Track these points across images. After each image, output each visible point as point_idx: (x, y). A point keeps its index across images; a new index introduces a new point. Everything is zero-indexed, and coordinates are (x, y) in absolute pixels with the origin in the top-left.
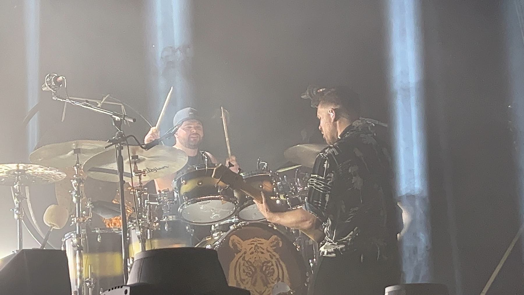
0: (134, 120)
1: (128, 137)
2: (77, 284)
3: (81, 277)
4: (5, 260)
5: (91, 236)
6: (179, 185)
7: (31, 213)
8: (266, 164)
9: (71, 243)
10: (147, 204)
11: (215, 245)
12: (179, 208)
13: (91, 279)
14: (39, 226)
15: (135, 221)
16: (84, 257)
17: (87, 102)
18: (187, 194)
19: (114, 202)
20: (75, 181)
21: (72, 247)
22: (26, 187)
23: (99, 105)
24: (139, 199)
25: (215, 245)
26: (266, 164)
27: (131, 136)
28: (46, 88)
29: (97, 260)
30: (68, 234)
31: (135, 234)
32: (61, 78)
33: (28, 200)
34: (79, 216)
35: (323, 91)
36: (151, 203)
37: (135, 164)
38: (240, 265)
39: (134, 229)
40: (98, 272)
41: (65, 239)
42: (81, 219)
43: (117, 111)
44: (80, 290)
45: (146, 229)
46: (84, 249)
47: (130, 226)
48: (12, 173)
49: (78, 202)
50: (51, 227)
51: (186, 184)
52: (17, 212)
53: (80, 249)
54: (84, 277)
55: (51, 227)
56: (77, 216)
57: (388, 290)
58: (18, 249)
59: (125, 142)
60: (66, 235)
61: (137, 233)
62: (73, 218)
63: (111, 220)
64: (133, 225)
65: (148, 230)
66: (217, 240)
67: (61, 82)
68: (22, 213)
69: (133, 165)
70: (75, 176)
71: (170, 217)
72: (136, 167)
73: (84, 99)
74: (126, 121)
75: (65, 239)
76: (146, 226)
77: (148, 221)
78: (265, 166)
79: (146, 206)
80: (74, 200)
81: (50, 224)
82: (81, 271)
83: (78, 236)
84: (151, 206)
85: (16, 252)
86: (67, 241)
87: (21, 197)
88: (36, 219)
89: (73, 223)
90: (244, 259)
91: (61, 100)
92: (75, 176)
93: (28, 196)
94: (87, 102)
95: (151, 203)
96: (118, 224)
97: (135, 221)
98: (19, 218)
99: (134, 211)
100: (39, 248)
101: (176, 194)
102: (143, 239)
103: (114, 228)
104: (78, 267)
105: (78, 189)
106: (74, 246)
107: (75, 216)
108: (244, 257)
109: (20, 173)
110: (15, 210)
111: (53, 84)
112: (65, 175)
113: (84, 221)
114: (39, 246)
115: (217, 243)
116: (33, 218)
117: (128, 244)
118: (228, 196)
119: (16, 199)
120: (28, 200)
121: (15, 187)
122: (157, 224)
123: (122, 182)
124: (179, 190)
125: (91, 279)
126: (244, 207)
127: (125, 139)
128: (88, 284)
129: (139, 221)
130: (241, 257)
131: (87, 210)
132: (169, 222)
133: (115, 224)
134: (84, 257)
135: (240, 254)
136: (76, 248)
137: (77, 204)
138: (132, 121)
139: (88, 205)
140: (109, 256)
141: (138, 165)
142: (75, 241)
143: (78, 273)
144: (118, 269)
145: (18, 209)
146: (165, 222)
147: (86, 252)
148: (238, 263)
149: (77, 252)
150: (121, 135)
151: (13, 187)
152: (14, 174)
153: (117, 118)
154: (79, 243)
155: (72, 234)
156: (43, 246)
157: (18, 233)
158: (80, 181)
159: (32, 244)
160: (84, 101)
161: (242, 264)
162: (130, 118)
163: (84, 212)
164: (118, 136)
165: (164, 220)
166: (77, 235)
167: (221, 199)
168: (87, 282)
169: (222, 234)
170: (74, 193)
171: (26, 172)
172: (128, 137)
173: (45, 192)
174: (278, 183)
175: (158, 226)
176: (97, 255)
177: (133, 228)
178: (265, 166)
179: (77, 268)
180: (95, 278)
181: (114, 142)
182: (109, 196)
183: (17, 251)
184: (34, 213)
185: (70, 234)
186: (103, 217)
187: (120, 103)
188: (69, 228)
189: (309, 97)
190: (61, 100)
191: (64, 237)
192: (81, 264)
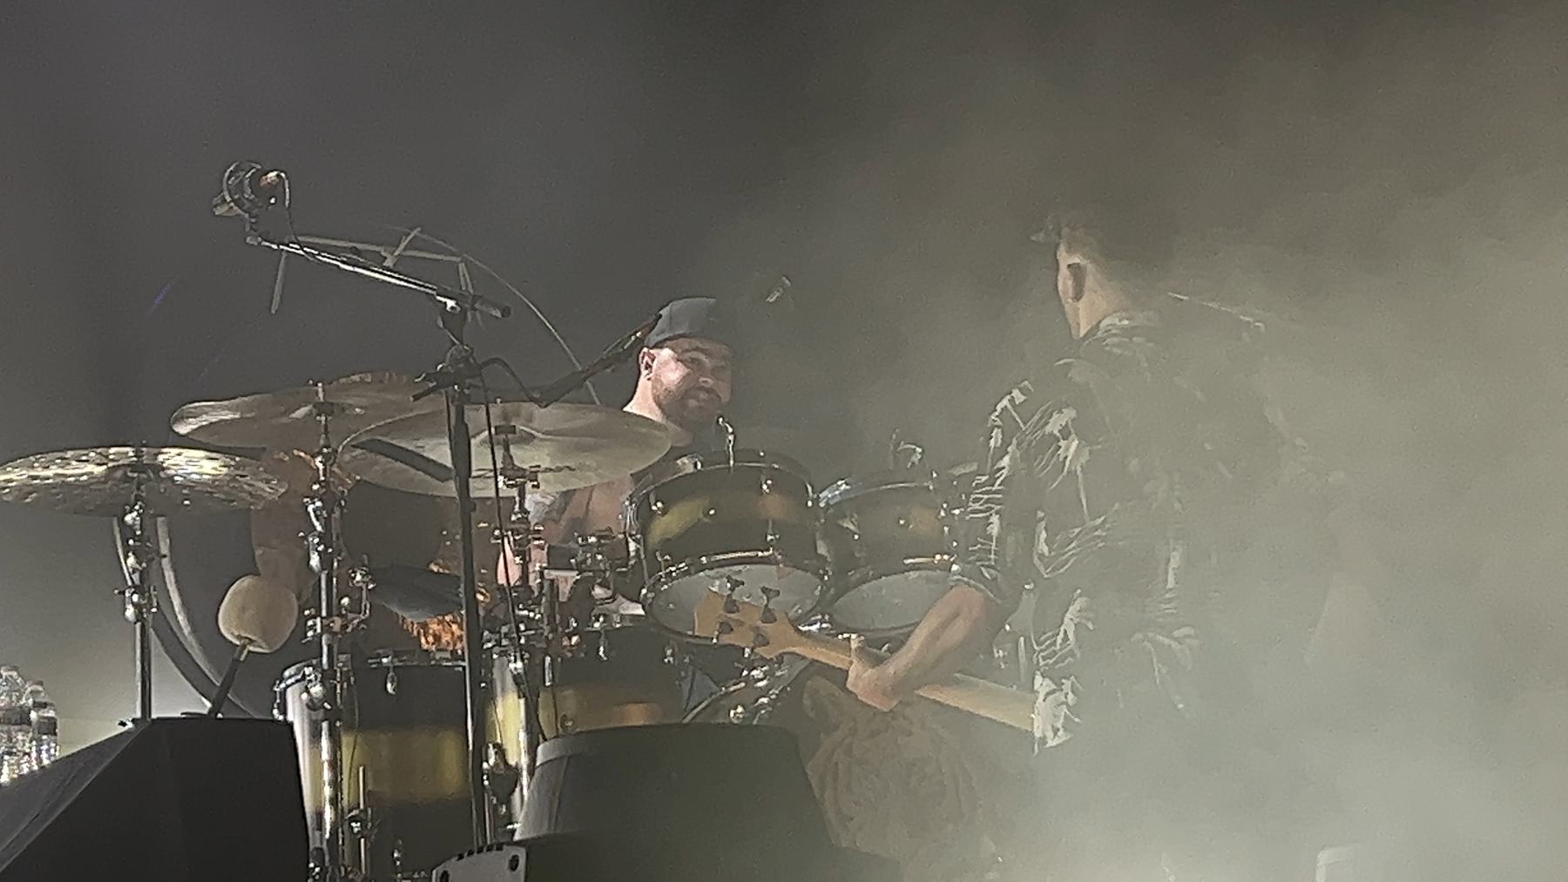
0: (506, 312)
3: (334, 801)
5: (365, 676)
6: (645, 517)
7: (176, 602)
9: (305, 696)
13: (365, 811)
15: (504, 629)
16: (346, 740)
18: (667, 545)
19: (435, 569)
22: (160, 519)
27: (494, 361)
28: (226, 208)
30: (292, 671)
32: (272, 175)
33: (165, 561)
34: (329, 614)
37: (507, 449)
39: (503, 654)
42: (337, 624)
48: (119, 474)
50: (244, 647)
51: (665, 512)
52: (135, 598)
53: (331, 717)
54: (345, 802)
56: (324, 613)
57: (1324, 857)
58: (138, 715)
59: (477, 382)
60: (287, 673)
61: (512, 666)
63: (425, 626)
64: (499, 643)
66: (764, 692)
68: (150, 598)
72: (508, 457)
77: (547, 629)
78: (916, 458)
80: (315, 561)
81: (239, 637)
82: (336, 784)
83: (326, 678)
85: (130, 725)
87: (147, 554)
88: (190, 620)
89: (310, 634)
93: (164, 550)
96: (446, 638)
97: (504, 629)
98: (139, 617)
100: (205, 712)
101: (632, 546)
102: (527, 687)
103: (438, 650)
104: (327, 775)
105: (327, 524)
106: (312, 706)
107: (319, 614)
113: (344, 627)
114: (206, 706)
115: (765, 700)
116: (180, 618)
117: (485, 699)
118: (797, 553)
119: (131, 560)
120: (165, 561)
121: (128, 518)
122: (575, 639)
124: (644, 530)
125: (365, 811)
126: (847, 590)
129: (518, 628)
131: (354, 593)
132: (609, 632)
133: (437, 638)
136: (321, 713)
138: (499, 315)
139: (359, 578)
142: (317, 690)
143: (327, 791)
145: (137, 589)
147: (349, 728)
149: (325, 725)
152: (127, 479)
153: (450, 303)
154: (330, 695)
155: (308, 671)
157: (138, 663)
159: (178, 701)
162: (495, 306)
163: (345, 601)
164: (455, 361)
165: (597, 625)
167: (777, 563)
168: (354, 819)
169: (778, 673)
172: (486, 364)
174: (957, 512)
175: (577, 644)
176: (382, 737)
178: (916, 458)
179: (320, 775)
181: (441, 381)
183: (134, 721)
184: (184, 604)
185: (299, 670)
186: (400, 613)
187: (453, 254)
188: (298, 650)
191: (282, 680)
192: (335, 764)
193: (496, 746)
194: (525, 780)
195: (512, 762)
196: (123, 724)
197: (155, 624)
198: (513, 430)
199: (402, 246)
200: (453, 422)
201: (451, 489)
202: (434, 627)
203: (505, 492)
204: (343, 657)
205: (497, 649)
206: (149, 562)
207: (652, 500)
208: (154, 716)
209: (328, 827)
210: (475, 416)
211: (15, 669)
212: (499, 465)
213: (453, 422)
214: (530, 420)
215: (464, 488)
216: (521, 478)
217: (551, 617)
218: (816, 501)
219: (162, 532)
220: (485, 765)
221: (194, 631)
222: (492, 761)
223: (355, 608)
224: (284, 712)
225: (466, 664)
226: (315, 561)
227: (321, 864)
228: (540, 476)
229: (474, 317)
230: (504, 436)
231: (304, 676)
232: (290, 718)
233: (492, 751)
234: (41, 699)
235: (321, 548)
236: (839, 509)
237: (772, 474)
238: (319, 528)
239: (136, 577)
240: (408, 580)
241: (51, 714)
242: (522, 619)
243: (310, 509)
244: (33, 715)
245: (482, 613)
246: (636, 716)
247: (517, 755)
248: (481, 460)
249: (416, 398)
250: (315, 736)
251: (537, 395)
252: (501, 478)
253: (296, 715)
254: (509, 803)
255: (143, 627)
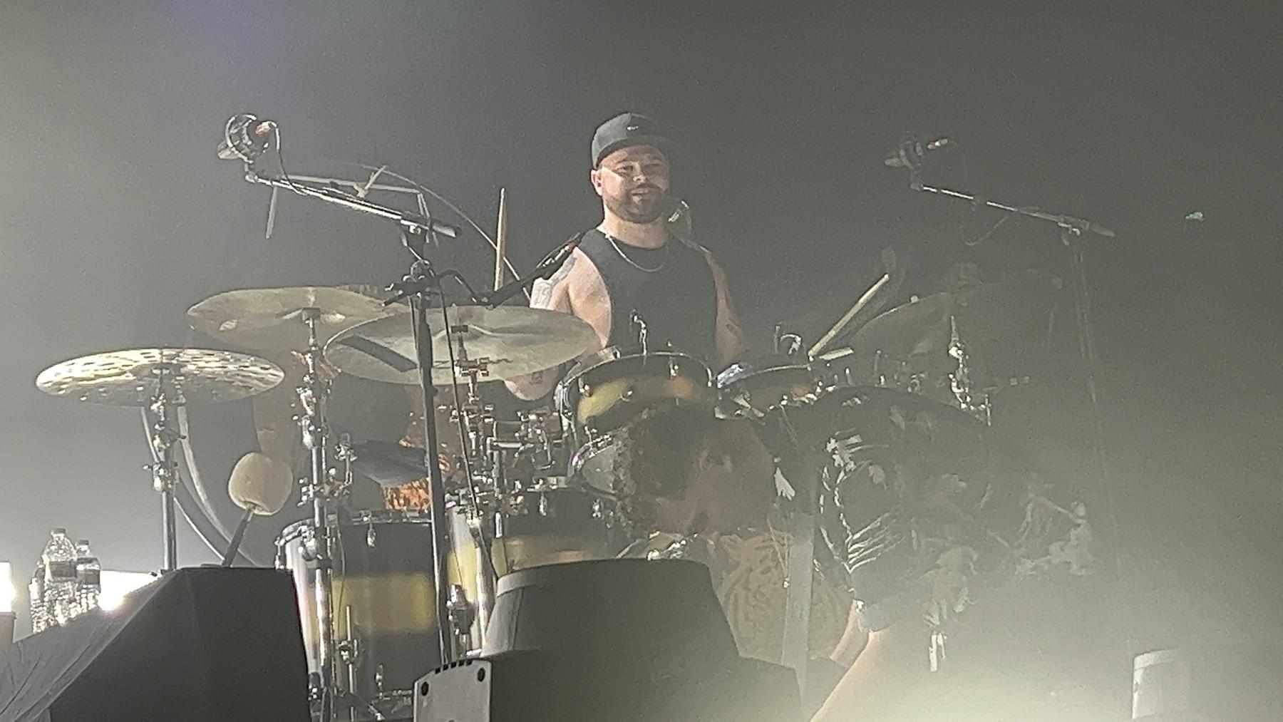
1: (441, 276)
2: (316, 655)
4: (135, 597)
5: (351, 533)
7: (195, 475)
8: (798, 339)
9: (301, 549)
10: (492, 447)
11: (671, 552)
12: (576, 459)
14: (215, 507)
15: (462, 492)
16: (336, 584)
17: (334, 185)
19: (404, 444)
20: (309, 392)
21: (302, 560)
23: (361, 194)
24: (472, 435)
25: (671, 552)
26: (798, 339)
27: (452, 272)
28: (228, 152)
29: (367, 592)
30: (290, 528)
31: (463, 525)
32: (265, 125)
33: (185, 442)
34: (320, 482)
35: (942, 146)
36: (502, 445)
37: (461, 345)
38: (736, 600)
39: (462, 512)
40: (369, 626)
41: (282, 542)
42: (327, 488)
43: (407, 207)
44: (327, 669)
45: (491, 514)
46: (333, 564)
47: (448, 505)
48: (146, 372)
49: (317, 442)
52: (162, 472)
53: (324, 565)
54: (336, 637)
55: (249, 510)
58: (166, 567)
60: (286, 531)
61: (469, 521)
62: (304, 485)
63: (397, 491)
65: (498, 516)
67: (267, 136)
68: (173, 475)
69: (456, 347)
70: (307, 379)
71: (553, 480)
72: (463, 352)
73: (327, 181)
74: (437, 233)
75: (282, 542)
76: (493, 504)
77: (497, 490)
79: (489, 452)
80: (307, 439)
81: (245, 502)
82: (328, 622)
83: (319, 533)
84: (504, 452)
85: (160, 575)
86: (288, 546)
87: (170, 436)
89: (304, 498)
90: (746, 588)
91: (268, 183)
92: (307, 379)
93: (184, 432)
94: (336, 186)
95: (502, 445)
97: (462, 492)
98: (165, 489)
99: (462, 466)
101: (565, 422)
102: (484, 539)
104: (321, 613)
106: (307, 558)
108: (747, 582)
109: (165, 372)
110: (156, 468)
111: (246, 140)
112: (282, 374)
113: (332, 492)
114: (219, 560)
115: (678, 546)
116: (198, 488)
117: (447, 546)
119: (157, 441)
120: (185, 442)
121: (154, 407)
122: (520, 499)
123: (431, 390)
124: (575, 409)
125: (352, 642)
127: (434, 281)
128: (345, 655)
130: (738, 580)
132: (547, 493)
133: (407, 501)
134: (334, 584)
135: (734, 575)
136: (315, 561)
137: (314, 452)
139: (343, 452)
140: (396, 582)
141: (465, 344)
142: (311, 544)
143: (321, 627)
144: (422, 615)
145: (162, 465)
146: (538, 494)
147: (339, 574)
148: (732, 597)
149: (318, 572)
150: (424, 270)
151: (148, 410)
154: (322, 547)
155: (304, 528)
156: (229, 558)
158: (317, 388)
159: (199, 554)
160: (325, 185)
161: (741, 601)
162: (446, 226)
163: (333, 471)
165: (537, 487)
166: (316, 529)
170: (305, 422)
171: (183, 370)
172: (441, 276)
173: (225, 423)
176: (367, 581)
177: (457, 509)
180: (364, 640)
182: (385, 427)
183: (162, 572)
184: (201, 477)
185: (295, 529)
187: (413, 187)
188: (294, 513)
189: (905, 162)
190: (268, 183)
192: (328, 604)
193: (457, 587)
194: (482, 613)
195: (470, 599)
196: (155, 575)
197: (177, 492)
198: (466, 329)
199: (373, 179)
200: (417, 322)
201: (416, 377)
202: (405, 492)
203: (461, 380)
204: (331, 517)
205: (457, 509)
206: (172, 442)
207: (581, 382)
208: (179, 567)
209: (323, 656)
210: (435, 317)
211: (63, 531)
212: (456, 358)
213: (417, 322)
214: (480, 319)
215: (428, 377)
216: (471, 367)
217: (500, 480)
218: (715, 383)
219: (182, 417)
220: (449, 603)
221: (209, 499)
222: (454, 599)
223: (341, 477)
224: (284, 562)
225: (432, 521)
226: (307, 439)
227: (318, 687)
228: (490, 367)
229: (431, 238)
230: (459, 332)
231: (300, 534)
232: (289, 566)
233: (454, 592)
234: (88, 555)
235: (312, 428)
236: (734, 388)
237: (679, 361)
238: (310, 412)
239: (161, 455)
240: (382, 454)
241: (96, 567)
242: (474, 484)
243: (302, 397)
244: (80, 568)
245: (444, 480)
246: (570, 557)
247: (477, 596)
248: (440, 353)
249: (386, 304)
250: (311, 581)
251: (485, 300)
252: (457, 369)
253: (295, 564)
254: (469, 633)
255: (168, 494)
